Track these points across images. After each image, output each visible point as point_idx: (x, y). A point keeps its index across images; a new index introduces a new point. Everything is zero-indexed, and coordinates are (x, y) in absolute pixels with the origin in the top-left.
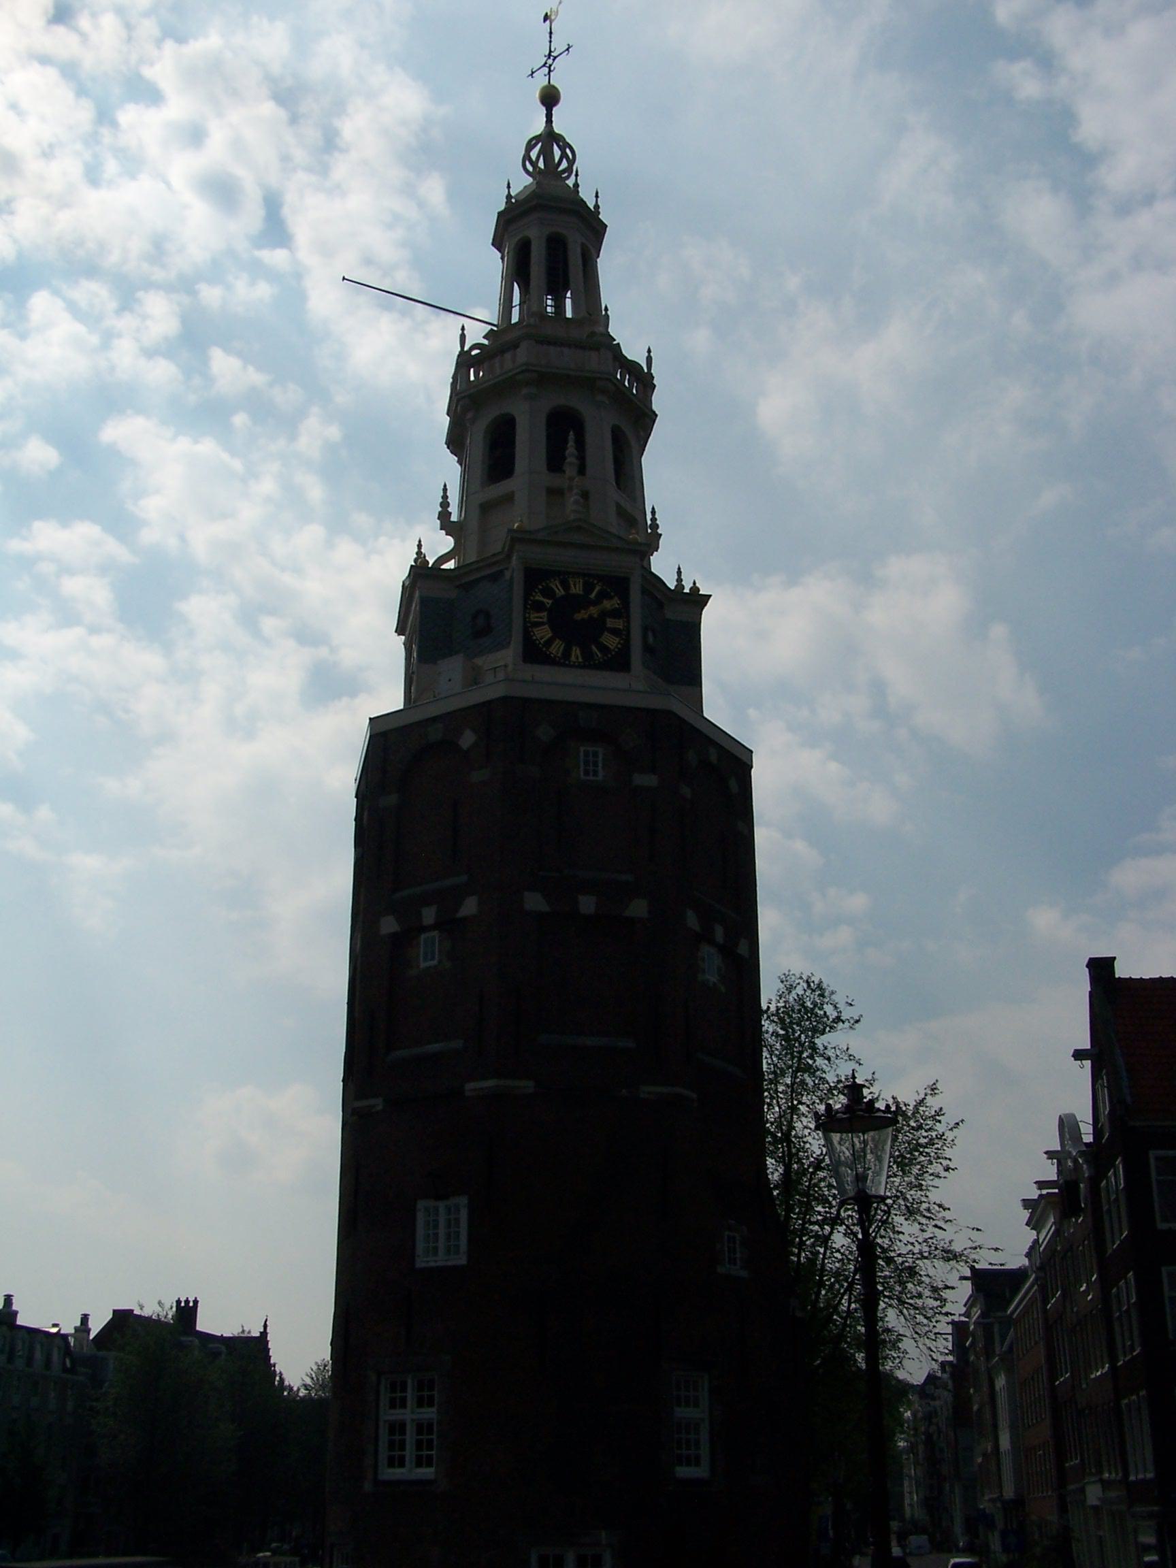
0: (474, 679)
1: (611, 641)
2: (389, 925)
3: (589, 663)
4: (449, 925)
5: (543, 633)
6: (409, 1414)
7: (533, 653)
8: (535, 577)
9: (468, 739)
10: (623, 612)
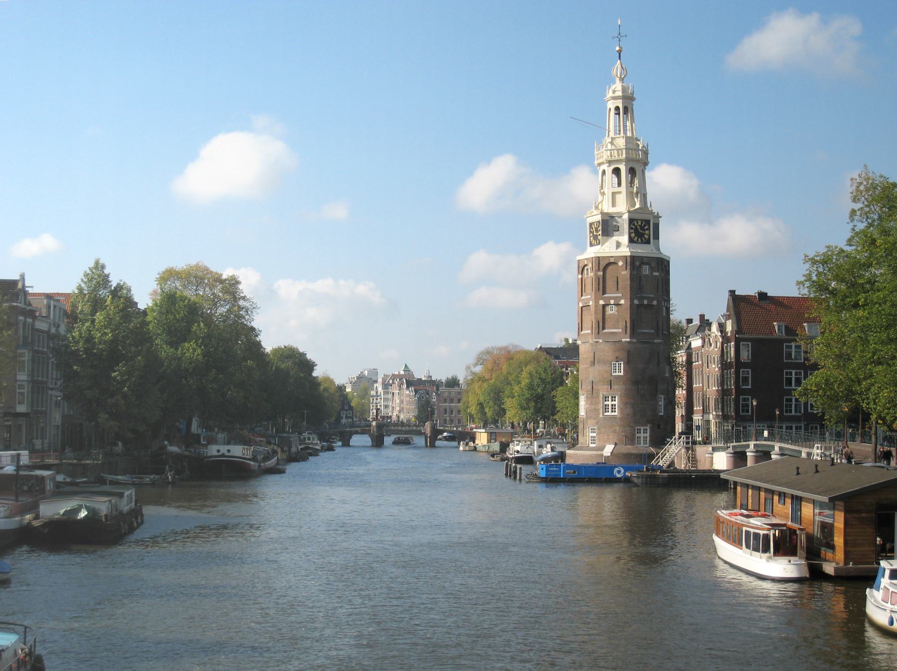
0: (618, 245)
1: (646, 237)
2: (602, 302)
3: (642, 242)
4: (617, 305)
5: (633, 235)
6: (610, 403)
7: (631, 240)
8: (631, 221)
9: (620, 263)
10: (649, 229)
